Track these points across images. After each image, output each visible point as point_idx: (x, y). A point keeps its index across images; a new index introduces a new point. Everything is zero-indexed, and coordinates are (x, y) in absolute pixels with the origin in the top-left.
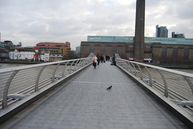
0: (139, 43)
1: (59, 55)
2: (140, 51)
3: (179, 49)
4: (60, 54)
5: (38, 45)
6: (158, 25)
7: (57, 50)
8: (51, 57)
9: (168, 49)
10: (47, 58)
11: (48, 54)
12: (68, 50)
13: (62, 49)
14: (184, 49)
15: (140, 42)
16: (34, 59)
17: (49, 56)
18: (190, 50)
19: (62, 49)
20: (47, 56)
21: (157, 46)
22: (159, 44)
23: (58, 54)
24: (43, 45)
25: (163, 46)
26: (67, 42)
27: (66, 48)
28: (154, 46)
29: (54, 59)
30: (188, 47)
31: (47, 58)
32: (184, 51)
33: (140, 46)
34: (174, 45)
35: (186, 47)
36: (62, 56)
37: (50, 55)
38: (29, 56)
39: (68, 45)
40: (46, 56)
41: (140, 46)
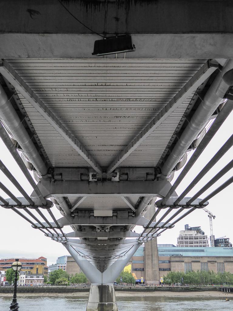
0: (150, 257)
1: (39, 277)
2: (152, 268)
3: (209, 264)
4: (34, 275)
6: (187, 225)
7: (30, 270)
8: (27, 280)
10: (22, 281)
11: (24, 276)
12: (45, 271)
13: (37, 269)
14: (216, 264)
15: (152, 255)
16: (4, 284)
17: (25, 278)
18: (225, 264)
19: (37, 269)
20: (22, 279)
21: (177, 259)
22: (182, 256)
23: (38, 276)
24: (6, 264)
26: (42, 257)
27: (43, 267)
28: (173, 259)
29: (31, 282)
31: (22, 281)
33: (152, 260)
34: (202, 257)
36: (43, 277)
37: (26, 277)
39: (43, 261)
41: (152, 260)
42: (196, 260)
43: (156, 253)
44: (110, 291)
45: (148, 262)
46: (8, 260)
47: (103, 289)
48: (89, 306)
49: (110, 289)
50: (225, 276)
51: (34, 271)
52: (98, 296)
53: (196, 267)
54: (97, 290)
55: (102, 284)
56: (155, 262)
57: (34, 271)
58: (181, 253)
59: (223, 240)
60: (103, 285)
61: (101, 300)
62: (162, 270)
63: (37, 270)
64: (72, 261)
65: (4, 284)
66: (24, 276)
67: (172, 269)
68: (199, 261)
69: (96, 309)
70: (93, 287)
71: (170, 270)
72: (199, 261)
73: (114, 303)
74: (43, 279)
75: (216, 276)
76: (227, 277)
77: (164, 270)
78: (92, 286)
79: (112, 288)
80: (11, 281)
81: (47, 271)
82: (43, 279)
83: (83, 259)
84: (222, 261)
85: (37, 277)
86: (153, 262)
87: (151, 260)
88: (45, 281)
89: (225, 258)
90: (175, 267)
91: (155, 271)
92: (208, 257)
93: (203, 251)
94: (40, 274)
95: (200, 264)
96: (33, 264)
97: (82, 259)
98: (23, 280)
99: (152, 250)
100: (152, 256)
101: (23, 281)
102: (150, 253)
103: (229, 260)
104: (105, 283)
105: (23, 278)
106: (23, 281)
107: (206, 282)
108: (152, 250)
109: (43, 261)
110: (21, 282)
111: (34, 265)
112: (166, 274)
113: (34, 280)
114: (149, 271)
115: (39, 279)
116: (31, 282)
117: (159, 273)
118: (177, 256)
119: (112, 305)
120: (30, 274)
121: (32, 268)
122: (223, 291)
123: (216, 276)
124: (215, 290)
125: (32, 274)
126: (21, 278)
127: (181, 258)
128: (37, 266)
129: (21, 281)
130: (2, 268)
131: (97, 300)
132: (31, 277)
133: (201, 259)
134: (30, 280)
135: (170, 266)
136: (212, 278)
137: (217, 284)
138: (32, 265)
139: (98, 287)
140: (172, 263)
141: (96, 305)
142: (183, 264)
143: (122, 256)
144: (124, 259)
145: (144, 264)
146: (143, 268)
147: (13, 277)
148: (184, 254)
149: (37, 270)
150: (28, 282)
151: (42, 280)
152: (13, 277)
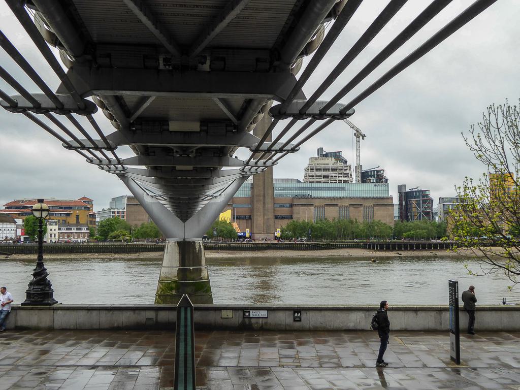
0: (261, 198)
1: (80, 229)
2: (264, 215)
3: (352, 209)
4: (73, 225)
5: (11, 208)
8: (61, 233)
9: (328, 209)
10: (53, 235)
11: (56, 227)
12: (91, 219)
13: (78, 216)
14: (362, 208)
15: (264, 196)
16: (22, 239)
17: (57, 231)
19: (78, 216)
20: (53, 231)
21: (303, 202)
22: (310, 197)
23: (79, 227)
25: (317, 203)
30: (371, 203)
31: (53, 235)
32: (362, 212)
33: (264, 203)
34: (340, 198)
35: (366, 204)
36: (87, 229)
37: (59, 229)
38: (5, 232)
39: (87, 204)
40: (50, 232)
41: (264, 203)
42: (332, 203)
43: (270, 192)
44: (197, 249)
45: (258, 206)
46: (26, 201)
47: (185, 247)
48: (163, 273)
49: (197, 247)
50: (373, 227)
51: (72, 220)
52: (177, 257)
53: (332, 214)
54: (177, 249)
55: (184, 239)
56: (269, 206)
57: (72, 220)
58: (309, 192)
59: (374, 173)
60: (186, 240)
61: (183, 261)
62: (278, 218)
63: (77, 218)
64: (135, 205)
65: (22, 239)
66: (56, 227)
67: (295, 216)
68: (337, 205)
69: (175, 277)
70: (170, 243)
71: (291, 217)
72: (337, 205)
73: (203, 268)
74: (89, 231)
75: (361, 227)
76: (376, 228)
77: (283, 218)
78: (168, 243)
79: (200, 246)
80: (34, 235)
81: (94, 220)
82: (89, 231)
83: (154, 200)
84: (371, 203)
85: (77, 229)
86: (266, 206)
87: (262, 203)
88: (91, 235)
89: (376, 200)
90: (299, 213)
91: (268, 219)
92: (351, 198)
93: (343, 189)
94: (83, 225)
95: (337, 208)
96: (71, 208)
97: (151, 201)
98: (53, 233)
99: (264, 188)
100: (265, 197)
101: (55, 235)
102: (262, 194)
103: (381, 202)
104: (190, 237)
105: (55, 230)
106: (55, 235)
107: (345, 235)
108: (264, 188)
109: (87, 204)
110: (51, 237)
111: (71, 210)
112: (285, 223)
113: (72, 233)
114: (259, 219)
115: (81, 233)
116: (69, 237)
117: (274, 222)
118: (303, 197)
119: (200, 270)
120: (65, 223)
121: (68, 215)
122: (370, 248)
123: (361, 227)
124: (357, 246)
125: (69, 224)
126: (51, 230)
127: (310, 199)
128: (78, 212)
129: (51, 234)
130: (17, 215)
131: (177, 263)
132: (67, 229)
133: (339, 201)
134: (66, 233)
135: (292, 212)
136: (354, 230)
137: (361, 238)
138: (69, 210)
139: (178, 243)
140: (294, 208)
141: (175, 271)
142: (312, 208)
143: (216, 197)
144: (219, 201)
145: (252, 210)
146: (250, 216)
147: (36, 228)
148: (314, 194)
149: (77, 218)
150: (64, 237)
151: (86, 233)
152: (36, 228)
